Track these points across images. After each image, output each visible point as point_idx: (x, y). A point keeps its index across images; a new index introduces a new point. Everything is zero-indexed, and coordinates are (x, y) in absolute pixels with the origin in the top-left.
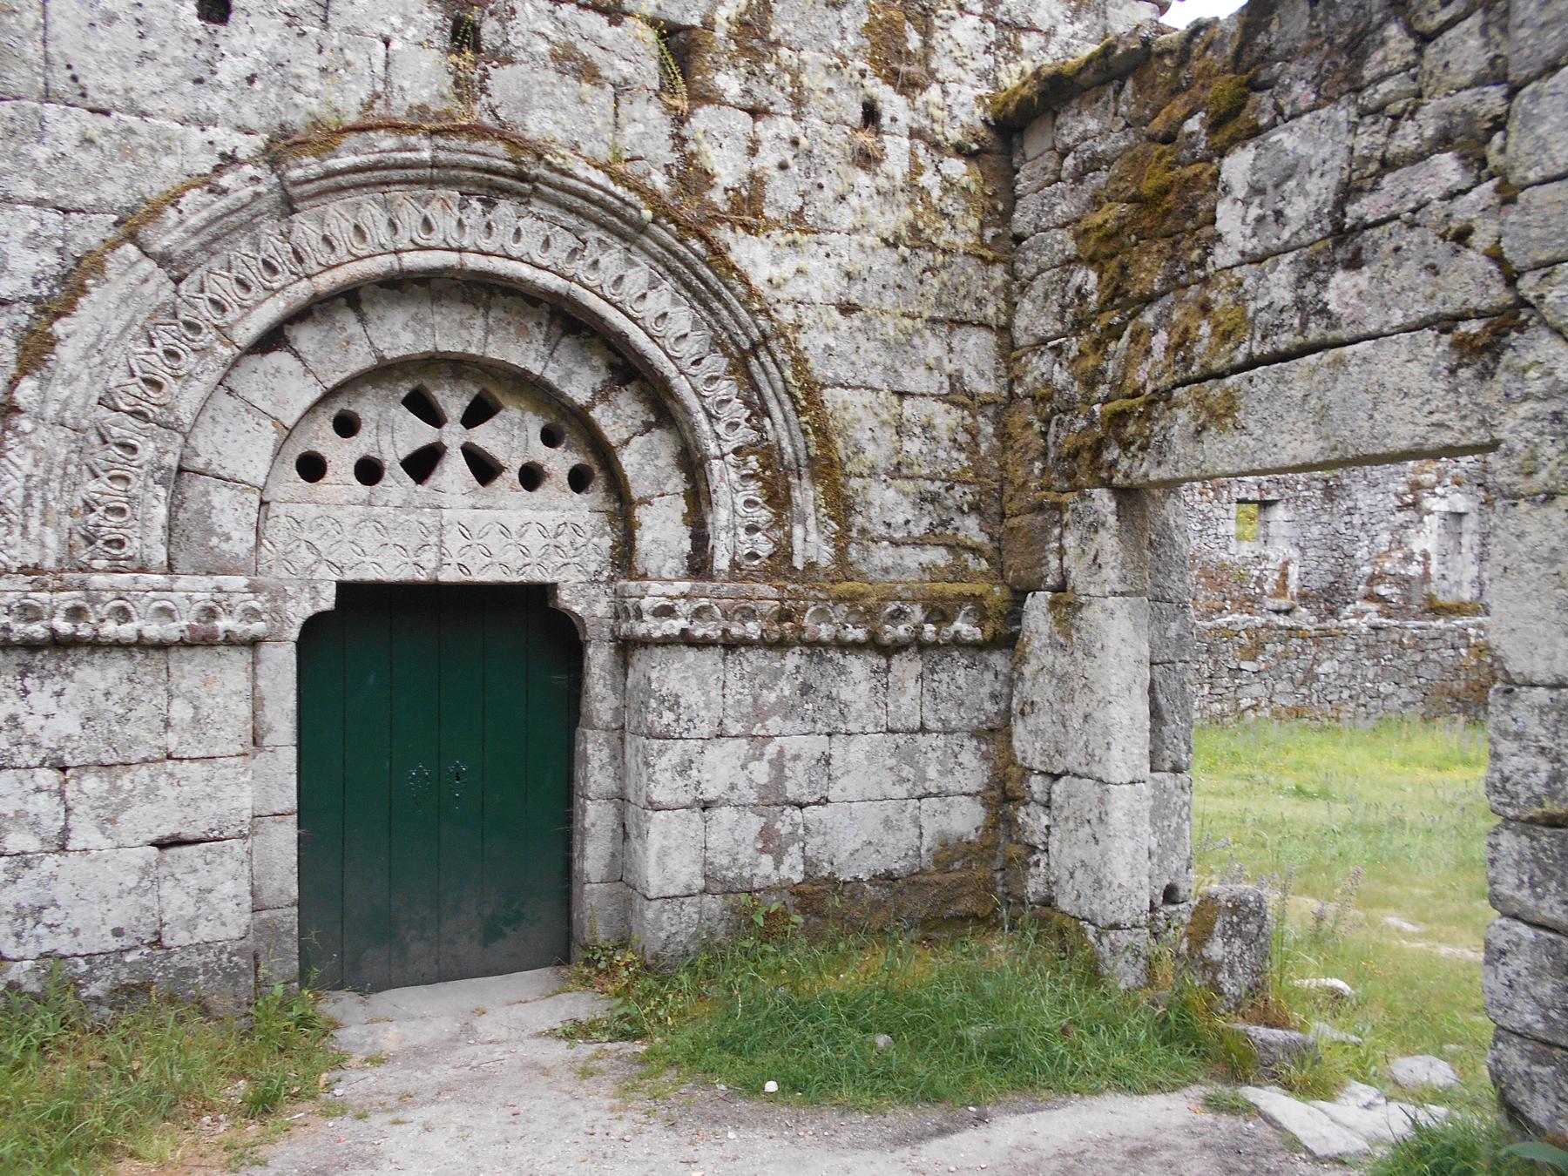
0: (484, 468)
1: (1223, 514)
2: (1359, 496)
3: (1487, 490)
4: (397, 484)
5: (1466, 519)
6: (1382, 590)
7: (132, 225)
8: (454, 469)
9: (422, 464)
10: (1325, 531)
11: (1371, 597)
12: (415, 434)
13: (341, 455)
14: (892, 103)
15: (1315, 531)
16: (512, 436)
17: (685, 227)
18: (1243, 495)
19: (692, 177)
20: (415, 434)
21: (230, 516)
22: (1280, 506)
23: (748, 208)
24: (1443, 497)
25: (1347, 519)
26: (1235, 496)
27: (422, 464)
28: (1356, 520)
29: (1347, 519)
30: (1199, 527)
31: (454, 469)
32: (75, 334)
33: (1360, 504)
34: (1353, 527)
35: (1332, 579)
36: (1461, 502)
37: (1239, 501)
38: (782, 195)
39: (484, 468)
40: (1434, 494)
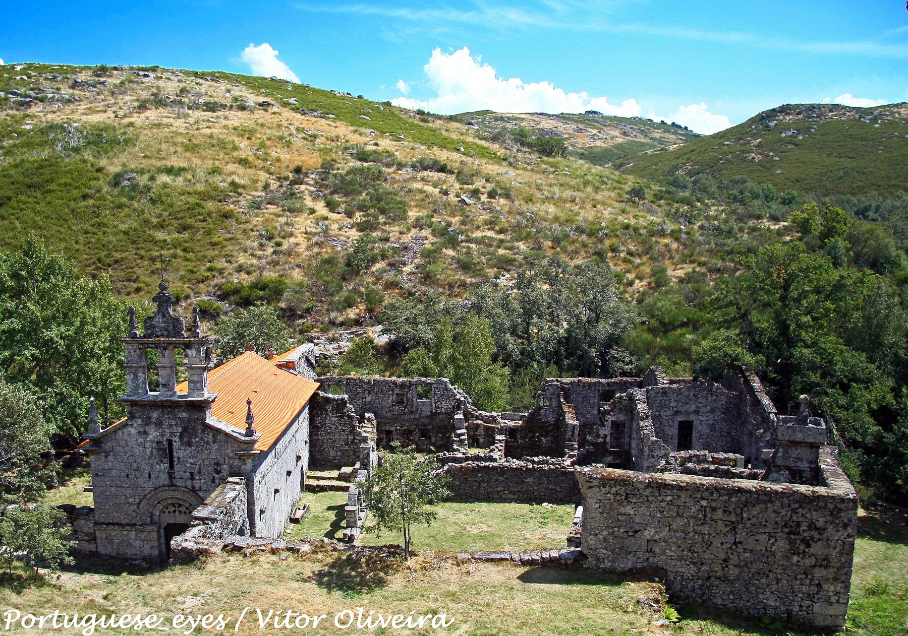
0: (180, 512)
4: (172, 514)
7: (145, 496)
8: (177, 513)
9: (175, 511)
12: (172, 509)
13: (167, 511)
14: (216, 476)
16: (183, 509)
17: (193, 490)
19: (193, 487)
20: (172, 509)
21: (156, 518)
23: (200, 490)
27: (175, 511)
31: (177, 513)
32: (141, 506)
38: (204, 488)
39: (180, 512)
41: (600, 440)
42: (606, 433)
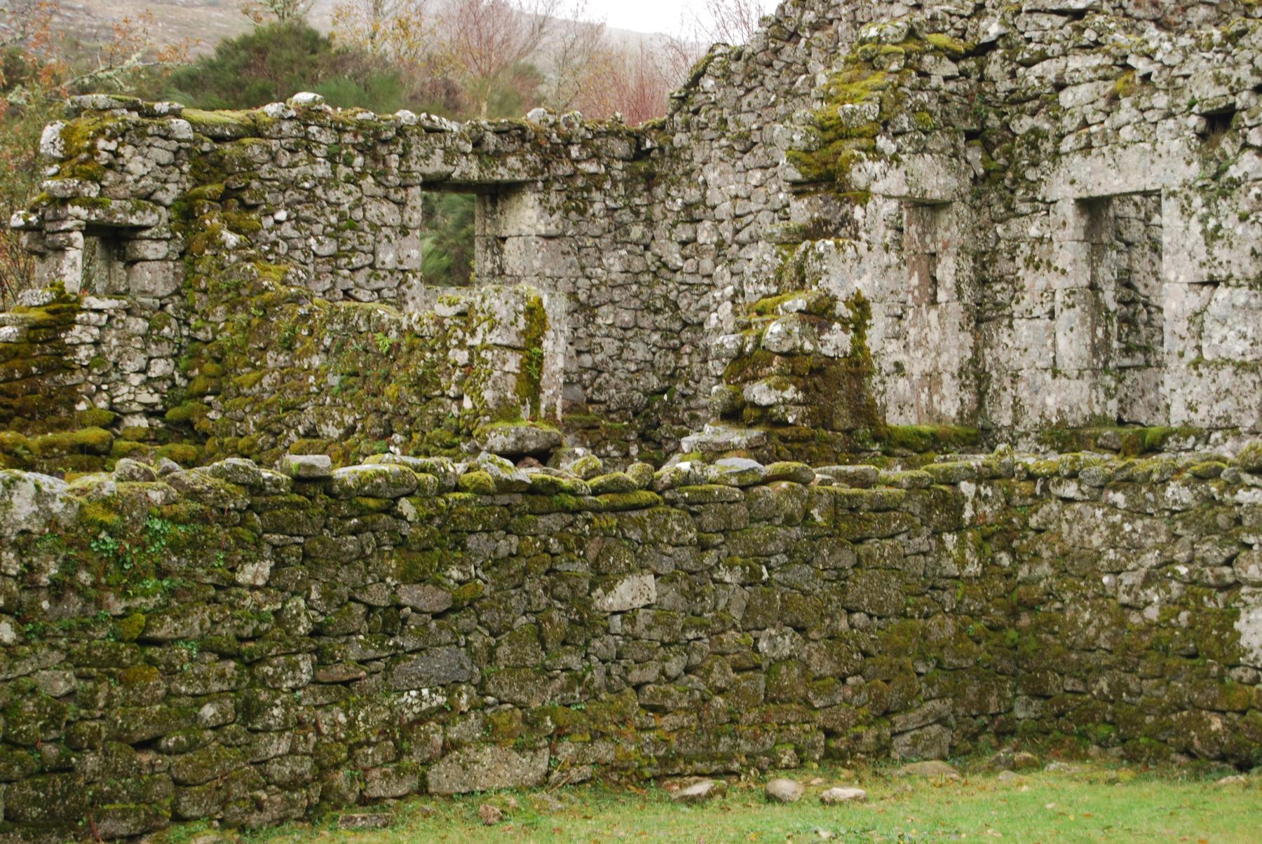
1: (389, 213)
2: (712, 175)
3: (988, 148)
5: (945, 218)
6: (760, 393)
10: (637, 264)
11: (733, 414)
15: (614, 263)
18: (437, 165)
22: (530, 198)
24: (895, 159)
25: (684, 232)
26: (419, 168)
28: (705, 235)
29: (684, 232)
30: (329, 247)
33: (713, 196)
34: (700, 251)
35: (655, 382)
36: (935, 178)
37: (430, 184)
40: (876, 153)
41: (837, 341)
42: (865, 284)
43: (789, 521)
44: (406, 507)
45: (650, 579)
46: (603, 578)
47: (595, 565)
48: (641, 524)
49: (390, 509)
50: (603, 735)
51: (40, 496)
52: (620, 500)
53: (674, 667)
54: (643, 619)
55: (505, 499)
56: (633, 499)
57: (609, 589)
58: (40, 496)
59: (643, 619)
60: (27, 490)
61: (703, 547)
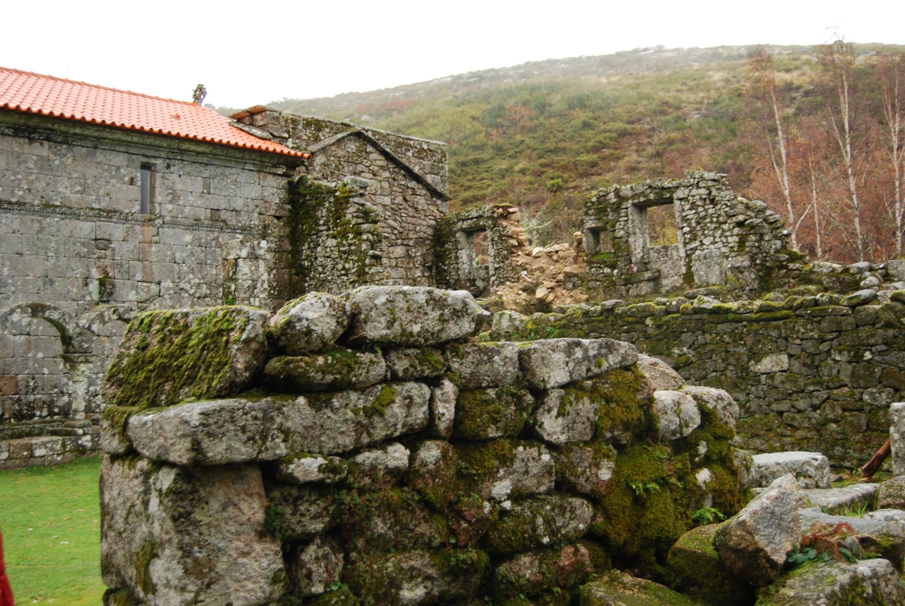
43: (888, 325)
44: (649, 321)
45: (784, 358)
46: (756, 356)
47: (750, 350)
48: (777, 328)
49: (642, 321)
50: (757, 435)
51: (511, 319)
52: (769, 315)
53: (801, 404)
54: (779, 378)
55: (697, 316)
56: (779, 314)
57: (758, 361)
58: (511, 319)
59: (779, 378)
60: (506, 317)
61: (822, 340)
